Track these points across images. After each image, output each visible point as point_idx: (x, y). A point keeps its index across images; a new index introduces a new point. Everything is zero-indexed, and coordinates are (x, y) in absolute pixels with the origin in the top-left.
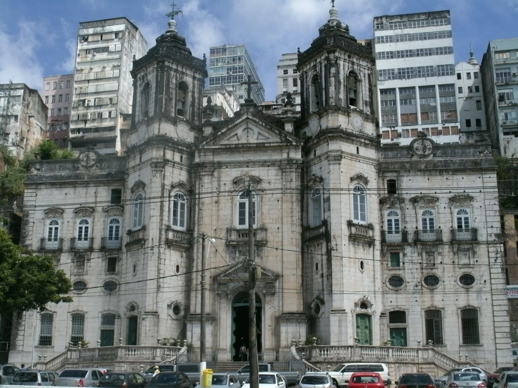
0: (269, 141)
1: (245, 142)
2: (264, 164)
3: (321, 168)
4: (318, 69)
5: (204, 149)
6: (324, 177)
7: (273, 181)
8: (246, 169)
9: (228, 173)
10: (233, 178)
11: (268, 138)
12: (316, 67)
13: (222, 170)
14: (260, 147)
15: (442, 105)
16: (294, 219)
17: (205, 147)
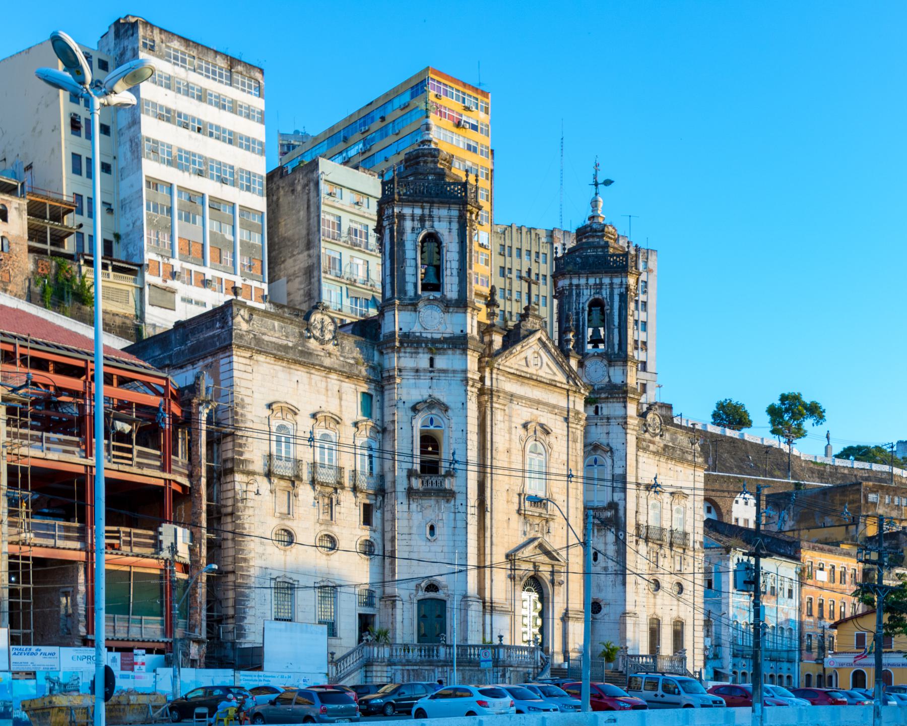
0: (557, 378)
1: (535, 372)
2: (552, 408)
3: (608, 433)
4: (605, 293)
5: (498, 369)
6: (613, 445)
7: (560, 437)
8: (535, 412)
9: (519, 412)
10: (523, 422)
11: (555, 374)
12: (601, 288)
13: (513, 406)
14: (552, 384)
15: (242, 242)
16: (579, 492)
17: (501, 367)
